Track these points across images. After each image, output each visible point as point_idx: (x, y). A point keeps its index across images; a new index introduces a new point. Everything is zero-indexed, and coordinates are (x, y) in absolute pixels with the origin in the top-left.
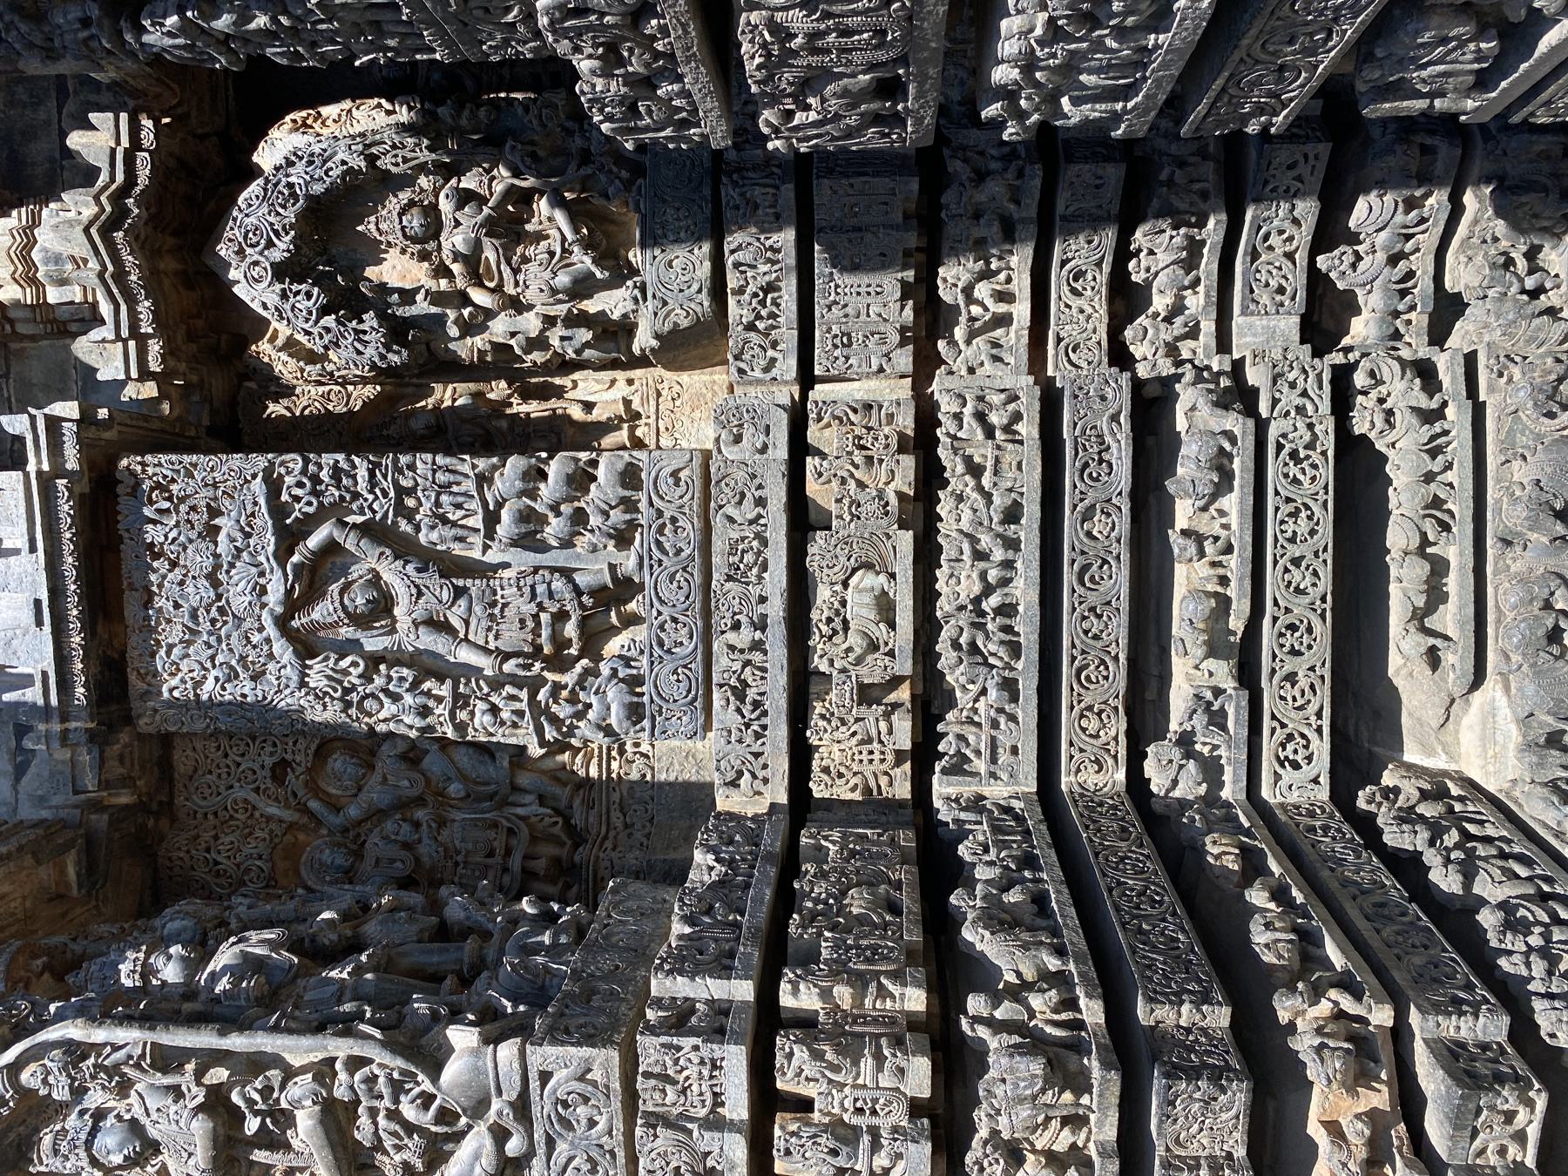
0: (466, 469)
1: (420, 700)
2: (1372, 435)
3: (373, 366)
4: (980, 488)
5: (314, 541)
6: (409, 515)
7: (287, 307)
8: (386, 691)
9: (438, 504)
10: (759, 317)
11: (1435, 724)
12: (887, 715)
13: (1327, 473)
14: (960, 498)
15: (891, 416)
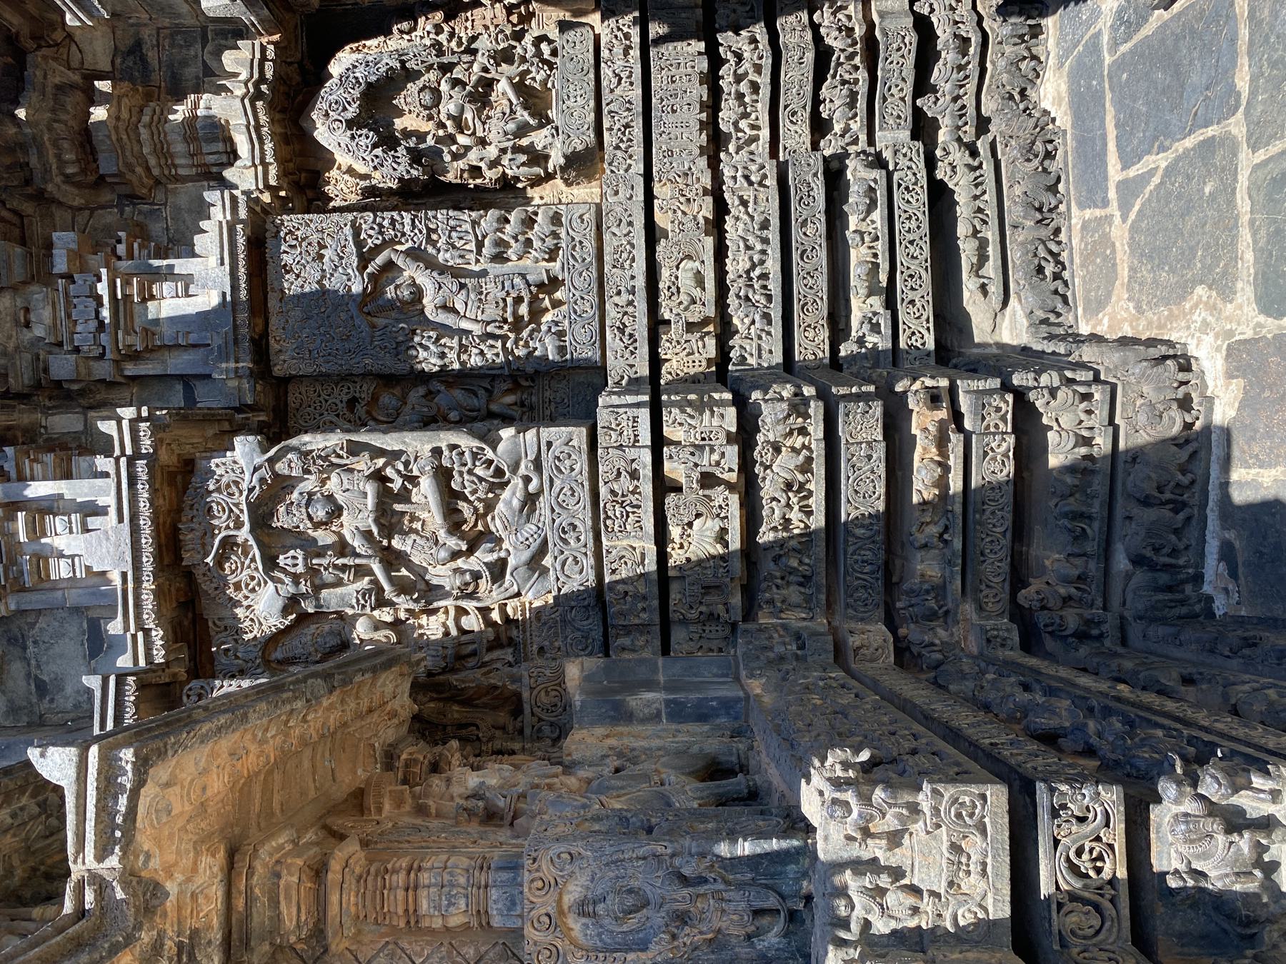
0: (466, 217)
1: (440, 349)
2: (946, 180)
3: (401, 180)
4: (748, 213)
5: (380, 260)
6: (434, 244)
7: (354, 144)
8: (421, 345)
9: (450, 237)
10: (622, 141)
11: (989, 331)
12: (702, 338)
13: (924, 197)
14: (737, 219)
15: (698, 179)
